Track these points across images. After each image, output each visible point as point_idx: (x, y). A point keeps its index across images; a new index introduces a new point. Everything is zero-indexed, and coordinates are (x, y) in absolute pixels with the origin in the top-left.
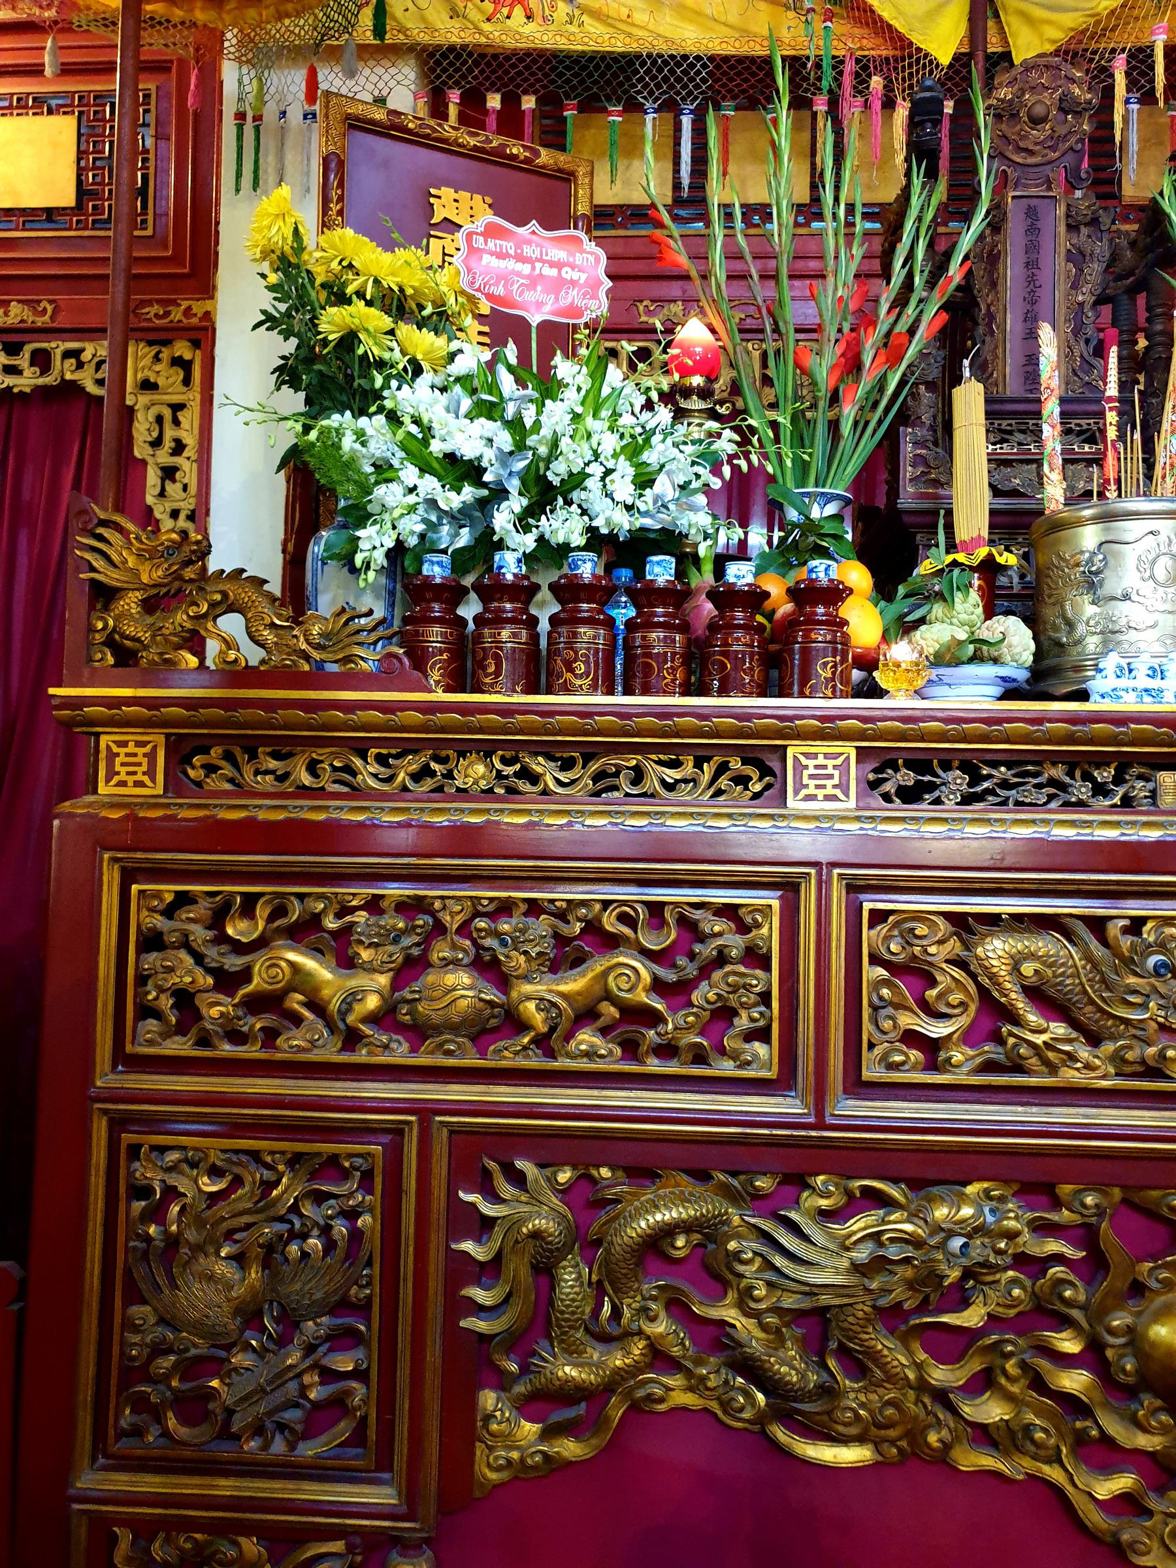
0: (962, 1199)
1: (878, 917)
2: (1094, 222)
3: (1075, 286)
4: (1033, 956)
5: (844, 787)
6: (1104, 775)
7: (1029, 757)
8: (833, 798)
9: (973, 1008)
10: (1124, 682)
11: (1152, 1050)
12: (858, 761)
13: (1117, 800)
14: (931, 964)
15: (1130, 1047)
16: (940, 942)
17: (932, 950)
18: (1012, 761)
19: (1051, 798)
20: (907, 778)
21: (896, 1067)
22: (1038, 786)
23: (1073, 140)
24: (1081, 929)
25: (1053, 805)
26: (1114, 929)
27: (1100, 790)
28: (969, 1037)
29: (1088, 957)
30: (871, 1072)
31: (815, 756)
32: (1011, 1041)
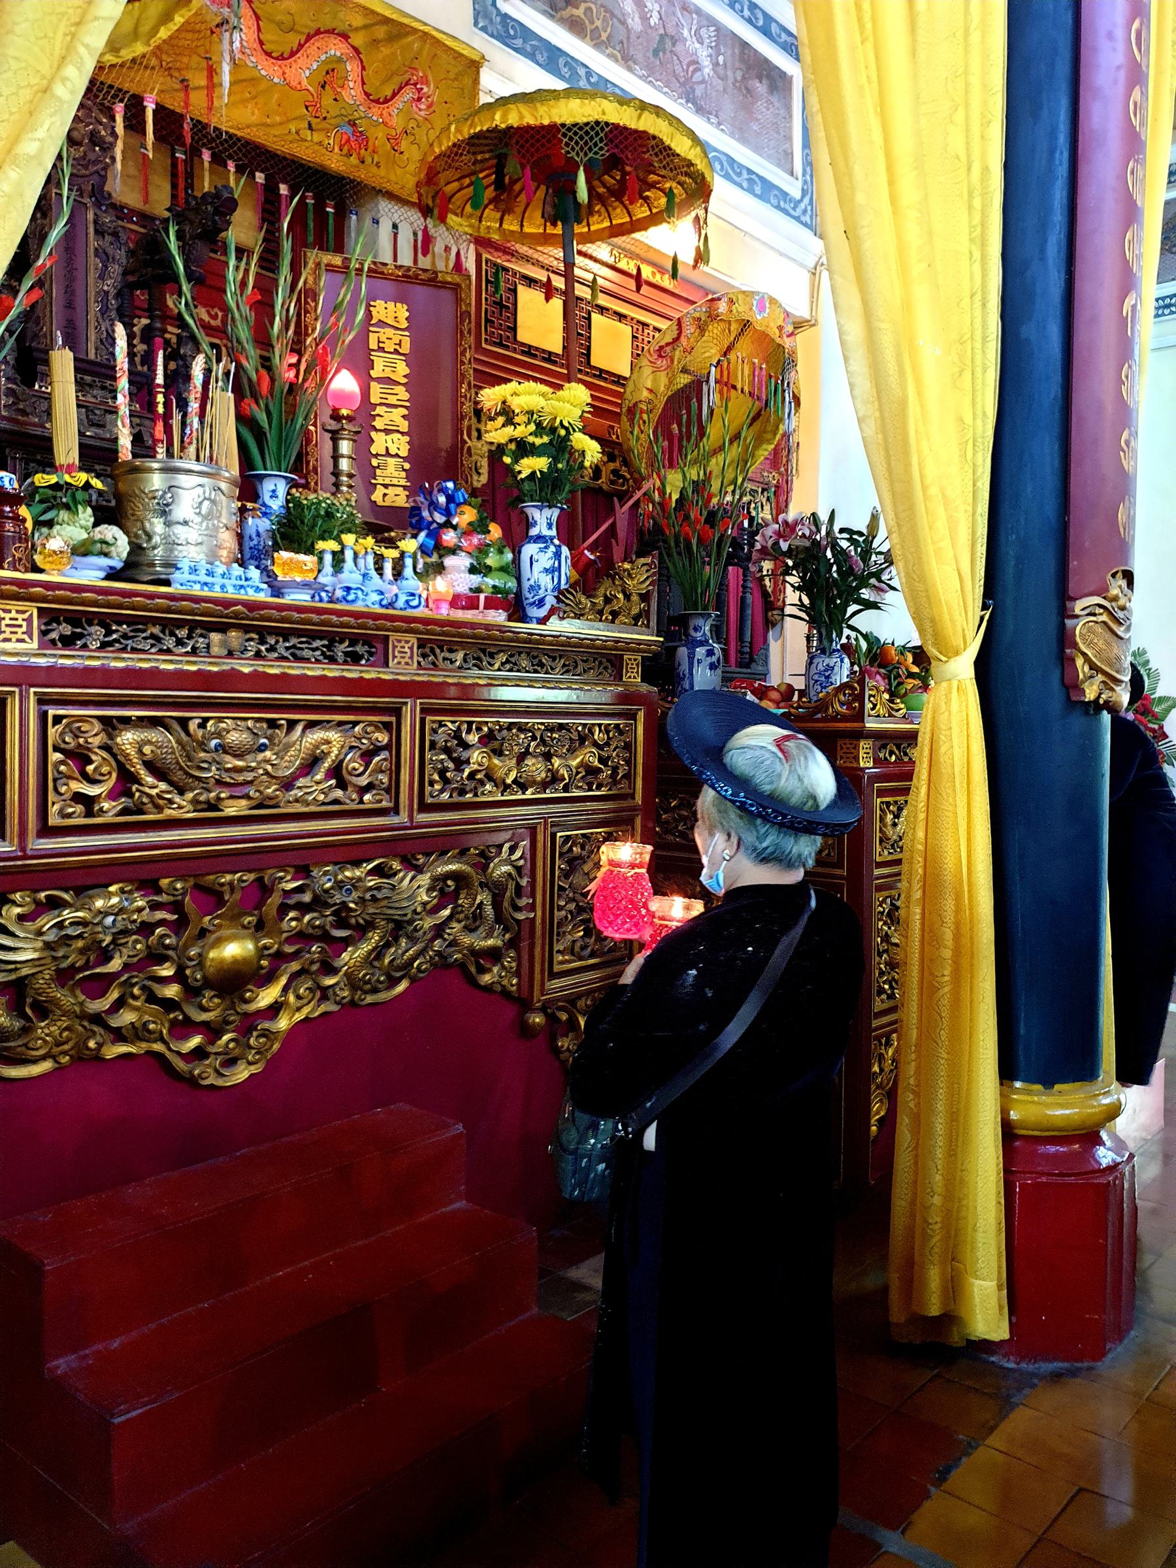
0: (110, 895)
1: (58, 719)
2: (115, 234)
3: (102, 277)
4: (149, 742)
5: (29, 633)
6: (182, 633)
7: (138, 620)
8: (22, 641)
9: (114, 775)
10: (193, 577)
11: (213, 795)
12: (39, 617)
13: (189, 649)
14: (89, 749)
15: (200, 794)
16: (96, 735)
17: (90, 740)
18: (130, 621)
19: (152, 646)
20: (67, 629)
21: (69, 816)
22: (145, 638)
23: (100, 166)
24: (176, 726)
25: (153, 650)
26: (193, 726)
27: (180, 642)
28: (112, 795)
29: (179, 742)
30: (54, 820)
31: (9, 611)
32: (137, 794)
